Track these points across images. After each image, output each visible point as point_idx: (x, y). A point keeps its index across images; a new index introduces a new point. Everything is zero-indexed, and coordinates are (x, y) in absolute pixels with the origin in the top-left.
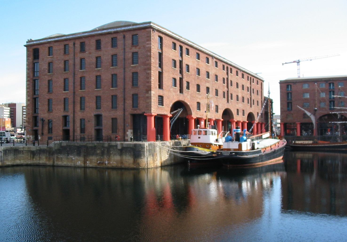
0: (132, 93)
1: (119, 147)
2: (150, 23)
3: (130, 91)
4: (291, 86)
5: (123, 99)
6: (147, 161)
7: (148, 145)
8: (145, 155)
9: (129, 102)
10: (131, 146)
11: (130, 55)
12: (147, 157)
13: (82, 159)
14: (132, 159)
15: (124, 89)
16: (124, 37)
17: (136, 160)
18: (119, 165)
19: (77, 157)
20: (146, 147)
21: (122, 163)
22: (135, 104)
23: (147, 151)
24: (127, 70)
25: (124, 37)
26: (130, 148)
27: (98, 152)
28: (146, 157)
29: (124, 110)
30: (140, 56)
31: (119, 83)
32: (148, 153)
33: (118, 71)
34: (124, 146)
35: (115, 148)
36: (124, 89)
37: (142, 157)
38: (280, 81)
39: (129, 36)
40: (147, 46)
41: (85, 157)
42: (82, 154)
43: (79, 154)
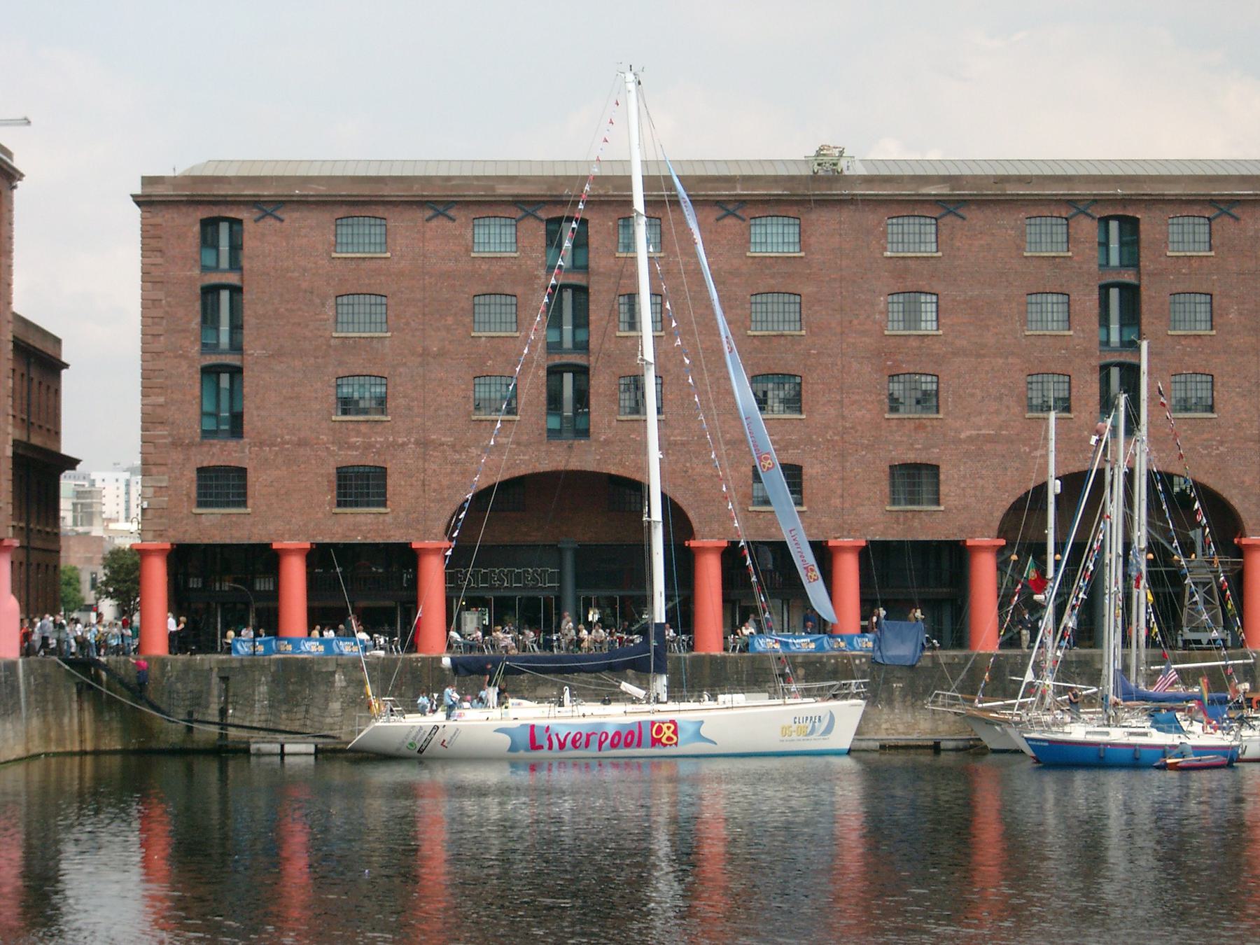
4: (235, 223)
38: (147, 181)
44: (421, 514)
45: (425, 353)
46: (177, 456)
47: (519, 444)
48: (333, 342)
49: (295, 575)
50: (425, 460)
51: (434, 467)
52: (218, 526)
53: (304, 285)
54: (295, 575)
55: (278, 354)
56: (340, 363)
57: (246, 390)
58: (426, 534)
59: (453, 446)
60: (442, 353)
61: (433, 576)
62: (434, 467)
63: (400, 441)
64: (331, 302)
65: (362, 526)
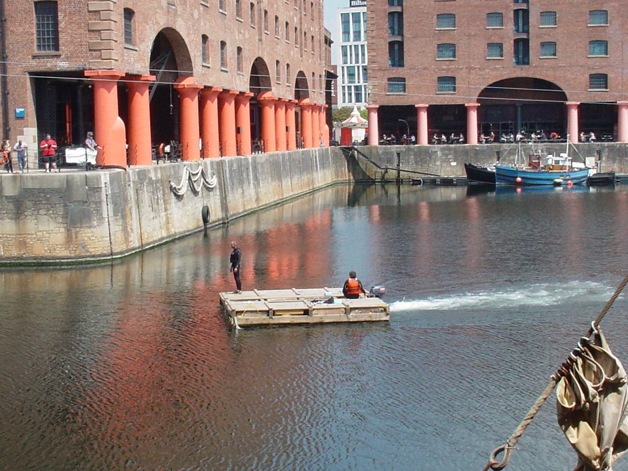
1: (9, 190)
6: (110, 236)
7: (108, 179)
8: (101, 214)
10: (56, 185)
12: (109, 221)
14: (62, 230)
17: (77, 233)
20: (103, 186)
21: (23, 244)
22: (50, 38)
23: (109, 200)
26: (53, 191)
28: (107, 220)
32: (111, 207)
34: (30, 185)
37: (95, 223)
44: (467, 95)
45: (469, 36)
46: (380, 74)
47: (503, 68)
48: (436, 32)
49: (423, 118)
50: (469, 74)
51: (473, 76)
52: (397, 99)
53: (425, 11)
54: (423, 118)
55: (416, 37)
56: (439, 39)
57: (405, 50)
58: (470, 101)
59: (480, 69)
60: (475, 35)
61: (473, 117)
62: (473, 76)
63: (460, 67)
64: (435, 17)
65: (447, 98)
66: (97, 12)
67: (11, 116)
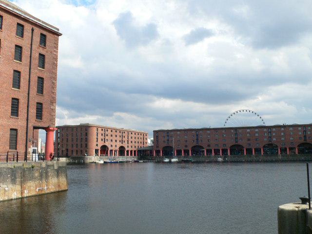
0: (37, 101)
2: (58, 30)
3: (35, 98)
5: (26, 105)
9: (33, 111)
11: (37, 55)
13: (18, 187)
15: (28, 94)
16: (33, 30)
18: (57, 190)
19: (11, 186)
21: (59, 186)
24: (32, 70)
25: (33, 30)
27: (37, 174)
29: (27, 120)
30: (47, 60)
31: (22, 84)
33: (23, 68)
35: (52, 168)
36: (28, 94)
39: (38, 31)
40: (55, 53)
41: (22, 183)
42: (18, 180)
43: (13, 181)
66: (53, 109)
67: (28, 141)
